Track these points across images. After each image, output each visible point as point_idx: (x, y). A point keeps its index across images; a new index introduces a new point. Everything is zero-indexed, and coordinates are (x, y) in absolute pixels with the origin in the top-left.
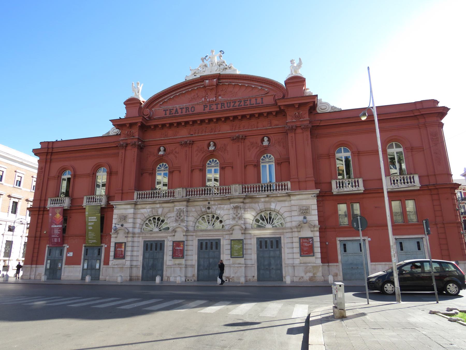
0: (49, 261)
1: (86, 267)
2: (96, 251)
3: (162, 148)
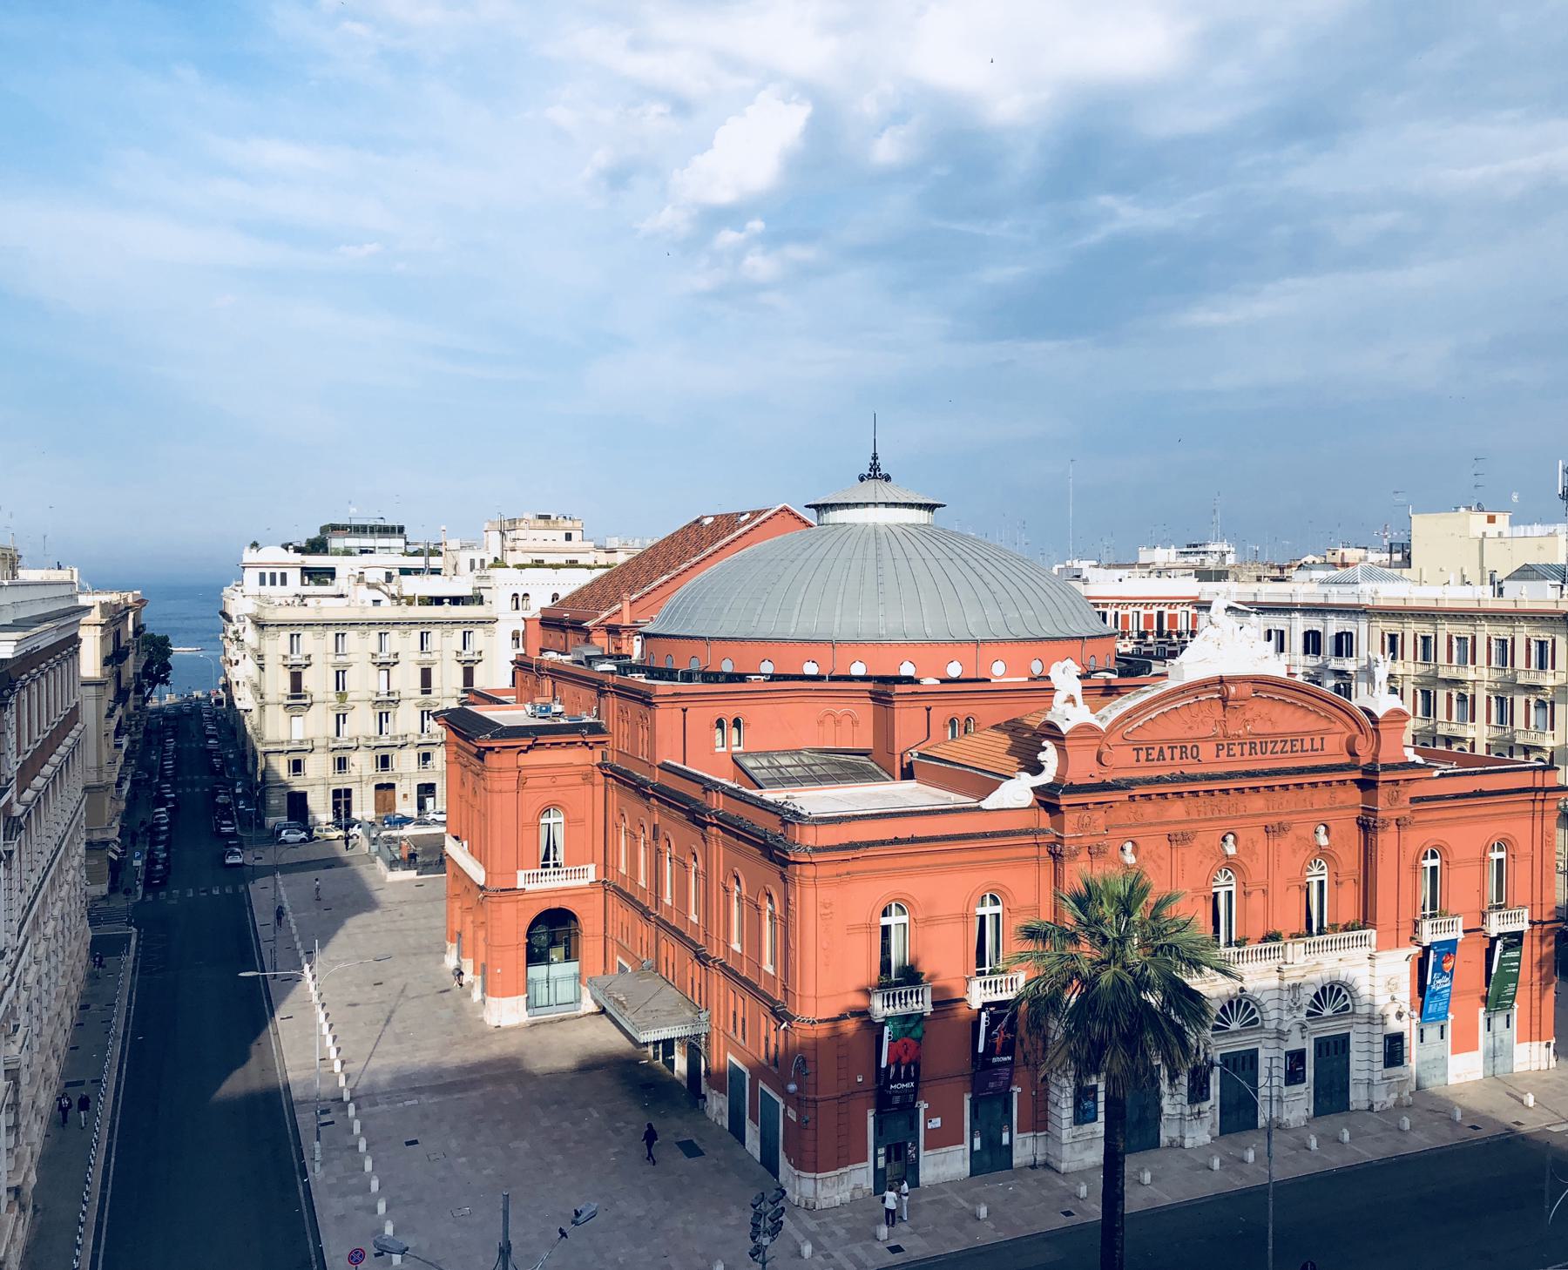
0: (881, 1151)
1: (977, 1146)
2: (999, 1106)
3: (1129, 846)
